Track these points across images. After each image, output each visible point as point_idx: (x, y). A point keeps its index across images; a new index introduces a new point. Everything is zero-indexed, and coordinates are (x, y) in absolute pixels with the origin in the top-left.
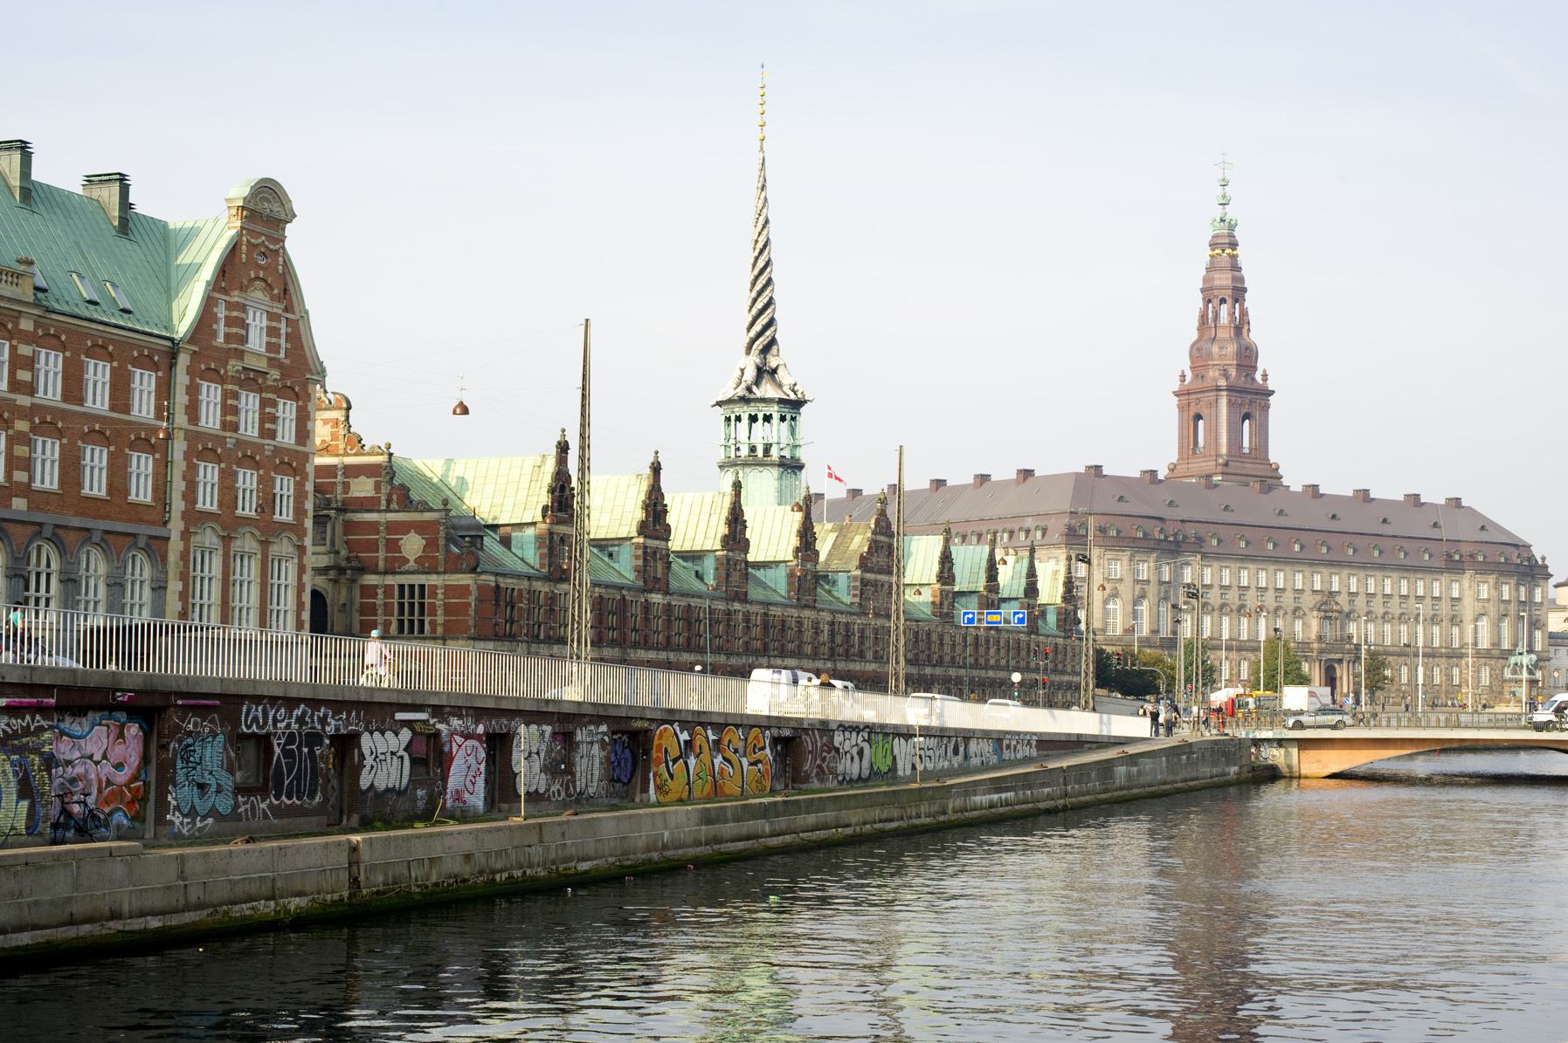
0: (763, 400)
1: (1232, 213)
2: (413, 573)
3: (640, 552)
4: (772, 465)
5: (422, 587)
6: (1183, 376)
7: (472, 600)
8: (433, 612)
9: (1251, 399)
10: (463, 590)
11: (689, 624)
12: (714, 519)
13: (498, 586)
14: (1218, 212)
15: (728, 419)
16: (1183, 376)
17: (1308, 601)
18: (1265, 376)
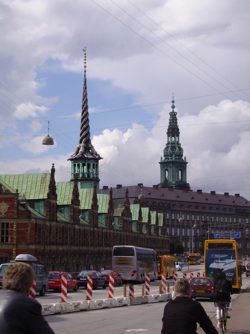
0: (87, 158)
1: (175, 110)
2: (4, 218)
3: (72, 210)
4: (91, 180)
5: (7, 224)
6: (162, 158)
7: (29, 228)
8: (12, 234)
9: (181, 165)
10: (26, 225)
11: (85, 236)
12: (88, 198)
13: (36, 223)
14: (171, 110)
15: (75, 165)
16: (162, 158)
17: (201, 224)
18: (185, 158)
